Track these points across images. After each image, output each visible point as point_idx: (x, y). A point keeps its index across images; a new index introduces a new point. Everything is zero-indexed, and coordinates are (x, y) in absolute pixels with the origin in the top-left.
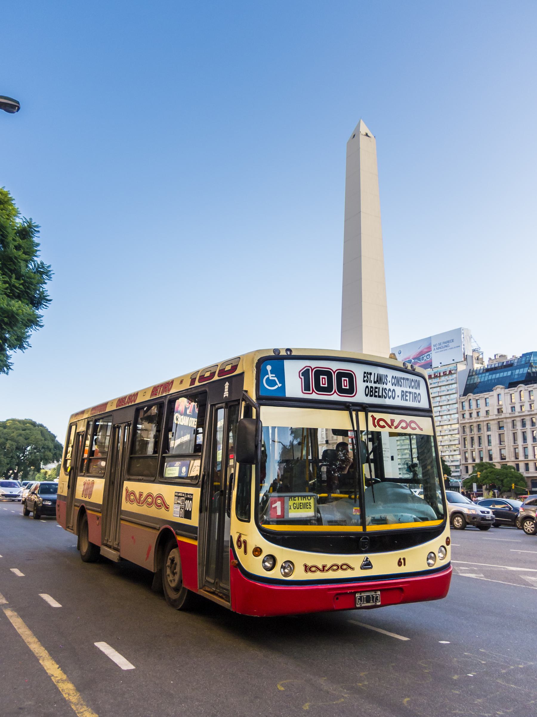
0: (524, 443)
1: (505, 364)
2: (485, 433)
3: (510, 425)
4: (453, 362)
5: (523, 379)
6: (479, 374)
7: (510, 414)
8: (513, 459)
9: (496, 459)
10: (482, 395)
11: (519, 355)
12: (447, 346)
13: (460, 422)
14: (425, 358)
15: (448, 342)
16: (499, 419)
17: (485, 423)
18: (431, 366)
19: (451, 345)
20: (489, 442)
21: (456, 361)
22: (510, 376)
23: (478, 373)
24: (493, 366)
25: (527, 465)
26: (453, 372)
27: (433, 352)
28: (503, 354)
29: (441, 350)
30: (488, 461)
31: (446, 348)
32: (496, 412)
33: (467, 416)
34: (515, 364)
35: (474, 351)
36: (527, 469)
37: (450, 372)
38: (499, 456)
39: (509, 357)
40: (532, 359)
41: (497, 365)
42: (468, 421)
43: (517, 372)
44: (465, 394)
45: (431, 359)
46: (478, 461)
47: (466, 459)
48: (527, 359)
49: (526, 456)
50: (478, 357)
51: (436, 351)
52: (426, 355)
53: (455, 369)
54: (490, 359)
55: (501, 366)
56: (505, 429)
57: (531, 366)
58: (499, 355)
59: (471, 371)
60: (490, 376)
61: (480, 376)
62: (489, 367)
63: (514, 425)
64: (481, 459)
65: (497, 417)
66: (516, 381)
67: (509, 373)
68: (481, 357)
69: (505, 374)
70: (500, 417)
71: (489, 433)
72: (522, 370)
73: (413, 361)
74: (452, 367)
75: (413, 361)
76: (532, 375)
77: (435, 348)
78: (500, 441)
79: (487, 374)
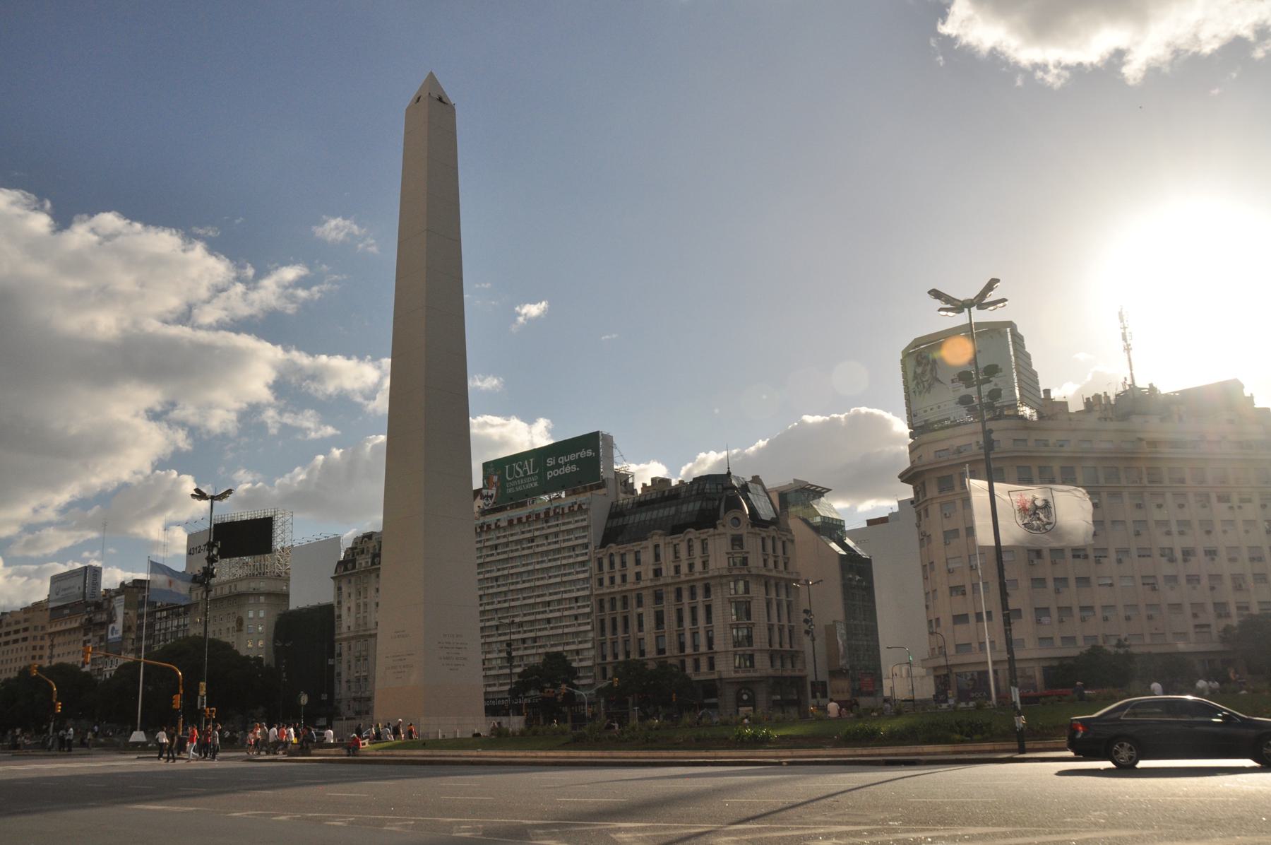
2: (634, 610)
3: (672, 597)
8: (676, 652)
9: (651, 652)
10: (629, 546)
17: (634, 594)
20: (641, 625)
30: (637, 657)
32: (651, 575)
33: (606, 582)
37: (580, 506)
38: (654, 649)
43: (684, 508)
44: (603, 545)
46: (621, 658)
47: (604, 657)
49: (696, 647)
54: (644, 485)
64: (627, 654)
67: (673, 509)
71: (640, 610)
72: (691, 507)
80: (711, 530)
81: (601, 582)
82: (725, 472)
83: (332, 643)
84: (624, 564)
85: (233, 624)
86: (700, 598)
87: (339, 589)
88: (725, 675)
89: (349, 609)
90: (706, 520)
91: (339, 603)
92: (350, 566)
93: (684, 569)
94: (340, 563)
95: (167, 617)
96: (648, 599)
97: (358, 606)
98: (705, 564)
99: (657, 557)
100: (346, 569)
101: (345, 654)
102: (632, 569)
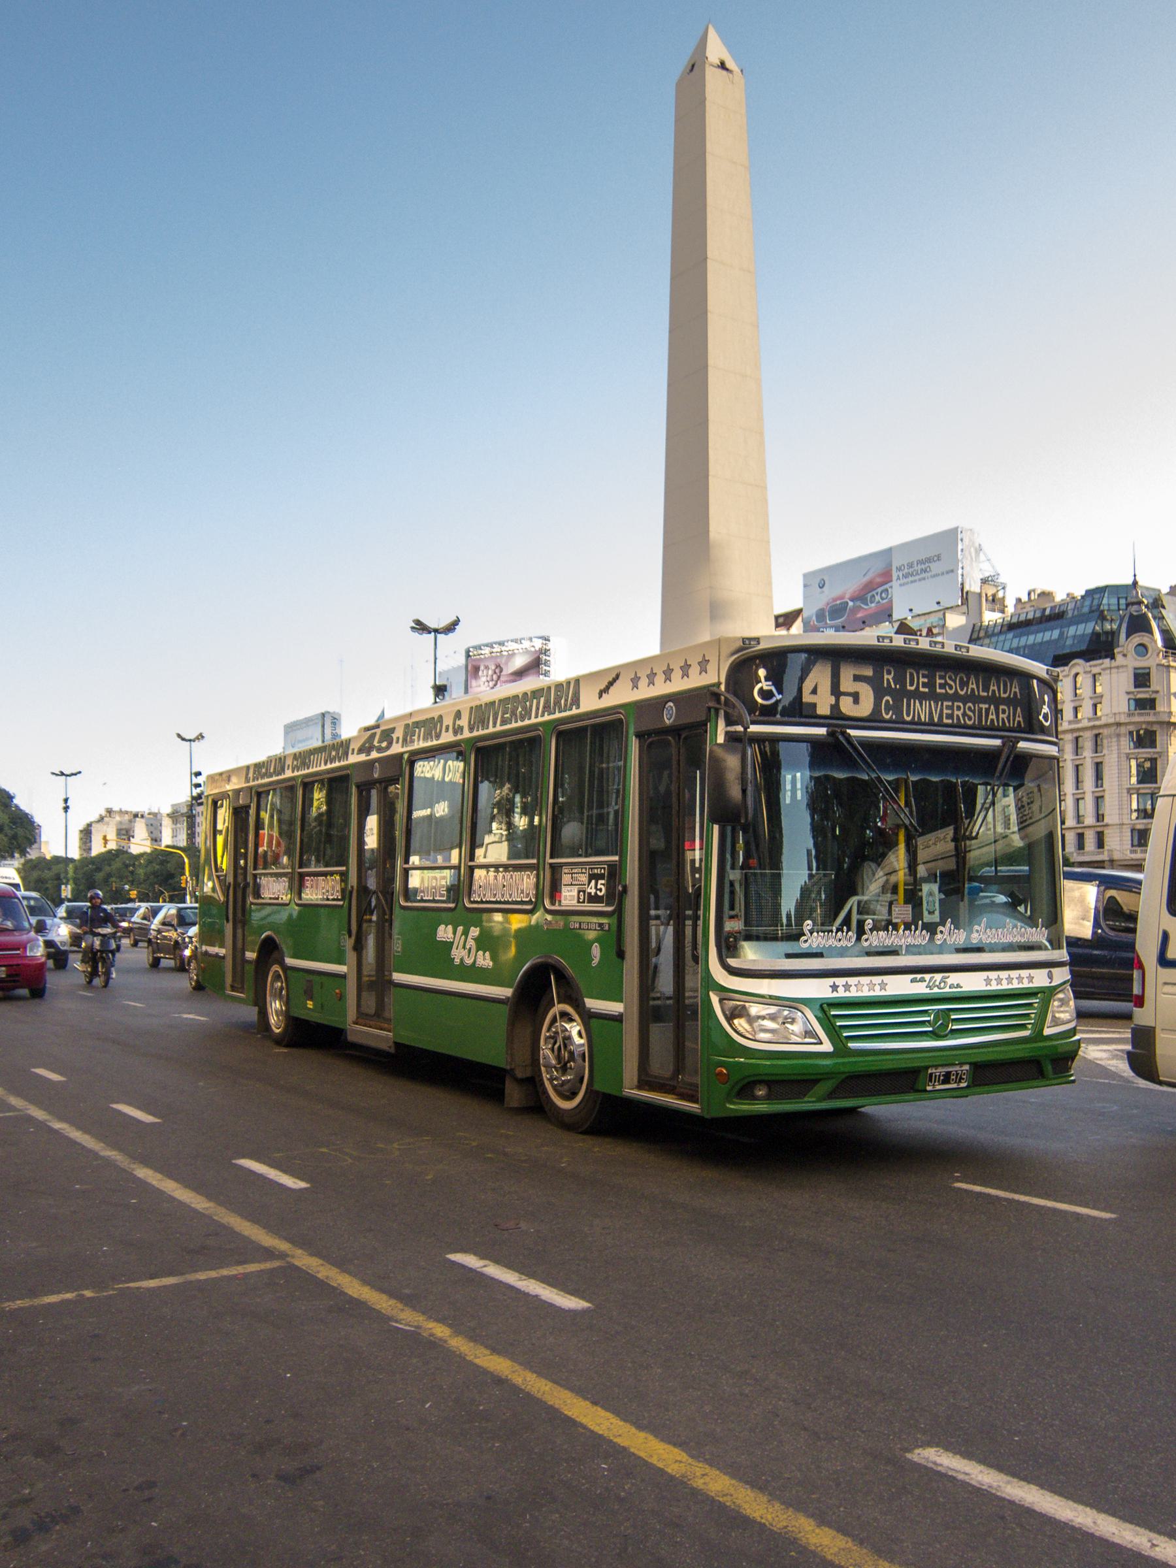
0: (1097, 786)
1: (1048, 612)
4: (937, 608)
5: (1083, 647)
6: (993, 635)
11: (1079, 592)
12: (925, 571)
14: (878, 598)
15: (929, 560)
18: (890, 616)
19: (935, 567)
21: (944, 604)
22: (1057, 641)
23: (990, 630)
24: (1022, 618)
25: (1081, 837)
26: (935, 631)
27: (895, 583)
28: (1047, 589)
31: (923, 575)
34: (1070, 615)
35: (984, 581)
36: (1081, 845)
39: (1060, 597)
40: (1105, 601)
41: (1030, 616)
43: (1072, 631)
45: (891, 601)
48: (1096, 602)
49: (1079, 818)
50: (994, 596)
51: (902, 581)
52: (879, 590)
53: (941, 623)
54: (1019, 600)
55: (1041, 617)
57: (1102, 617)
58: (1038, 592)
59: (977, 628)
60: (1016, 641)
61: (994, 639)
62: (1015, 620)
68: (1000, 595)
69: (1047, 636)
72: (1081, 627)
73: (851, 604)
74: (933, 620)
75: (851, 604)
76: (1103, 638)
78: (1078, 782)
79: (1010, 635)
80: (1108, 660)
82: (1130, 581)
86: (1088, 753)
88: (1116, 856)
90: (1100, 648)
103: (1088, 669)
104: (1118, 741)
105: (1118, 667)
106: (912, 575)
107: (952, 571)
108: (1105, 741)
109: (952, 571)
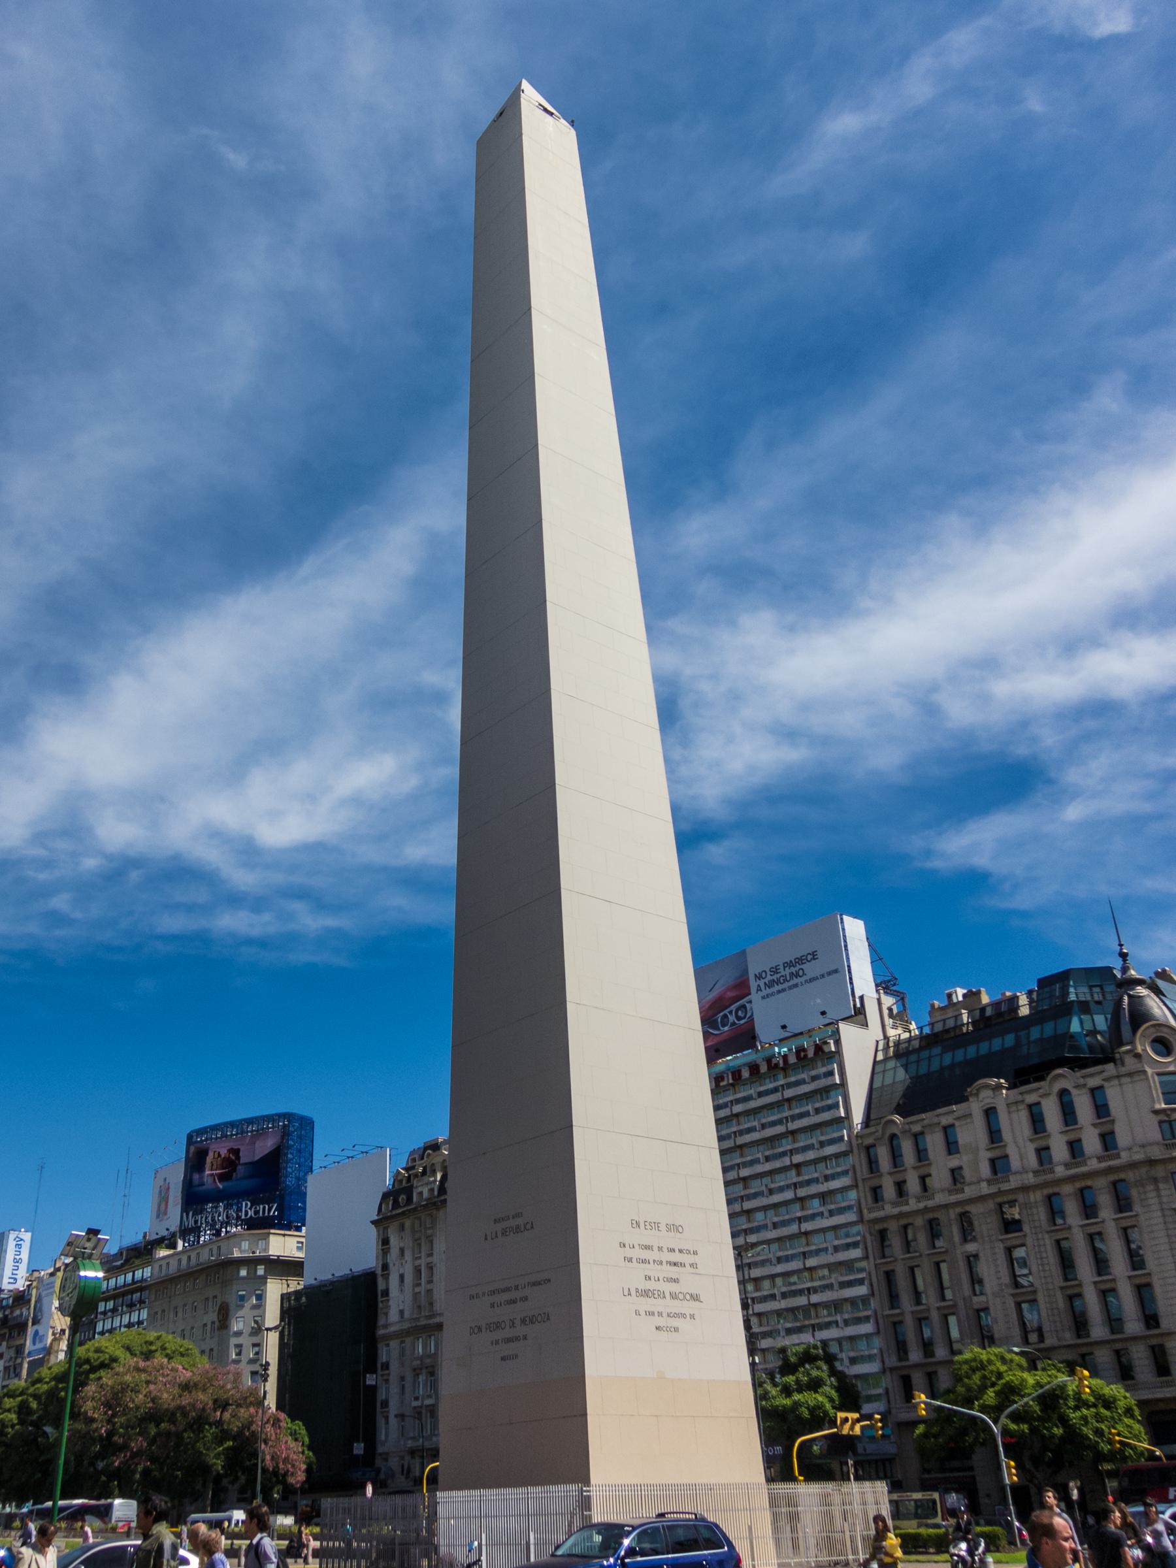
3: (1042, 1213)
7: (1036, 1173)
12: (797, 975)
13: (867, 1216)
14: (732, 1018)
15: (801, 960)
16: (1000, 1193)
17: (953, 1213)
19: (811, 969)
27: (755, 996)
29: (780, 987)
31: (795, 981)
32: (985, 1170)
33: (889, 1191)
42: (896, 1211)
52: (733, 1007)
56: (1026, 1228)
63: (1055, 1212)
65: (993, 1189)
66: (1035, 1061)
70: (1005, 1187)
71: (971, 1247)
77: (761, 983)
80: (1110, 1068)
81: (876, 1193)
83: (372, 1343)
84: (921, 1154)
85: (212, 1316)
86: (1107, 1213)
87: (385, 1242)
89: (402, 1277)
91: (385, 1267)
92: (402, 1198)
93: (1059, 1151)
94: (385, 1196)
95: (114, 1310)
96: (986, 1224)
97: (417, 1271)
98: (1108, 1140)
99: (994, 1135)
100: (396, 1205)
101: (394, 1366)
102: (940, 1165)
103: (1082, 1081)
104: (1158, 1190)
105: (1130, 1075)
106: (778, 982)
107: (836, 971)
108: (1134, 1193)
109: (836, 971)
